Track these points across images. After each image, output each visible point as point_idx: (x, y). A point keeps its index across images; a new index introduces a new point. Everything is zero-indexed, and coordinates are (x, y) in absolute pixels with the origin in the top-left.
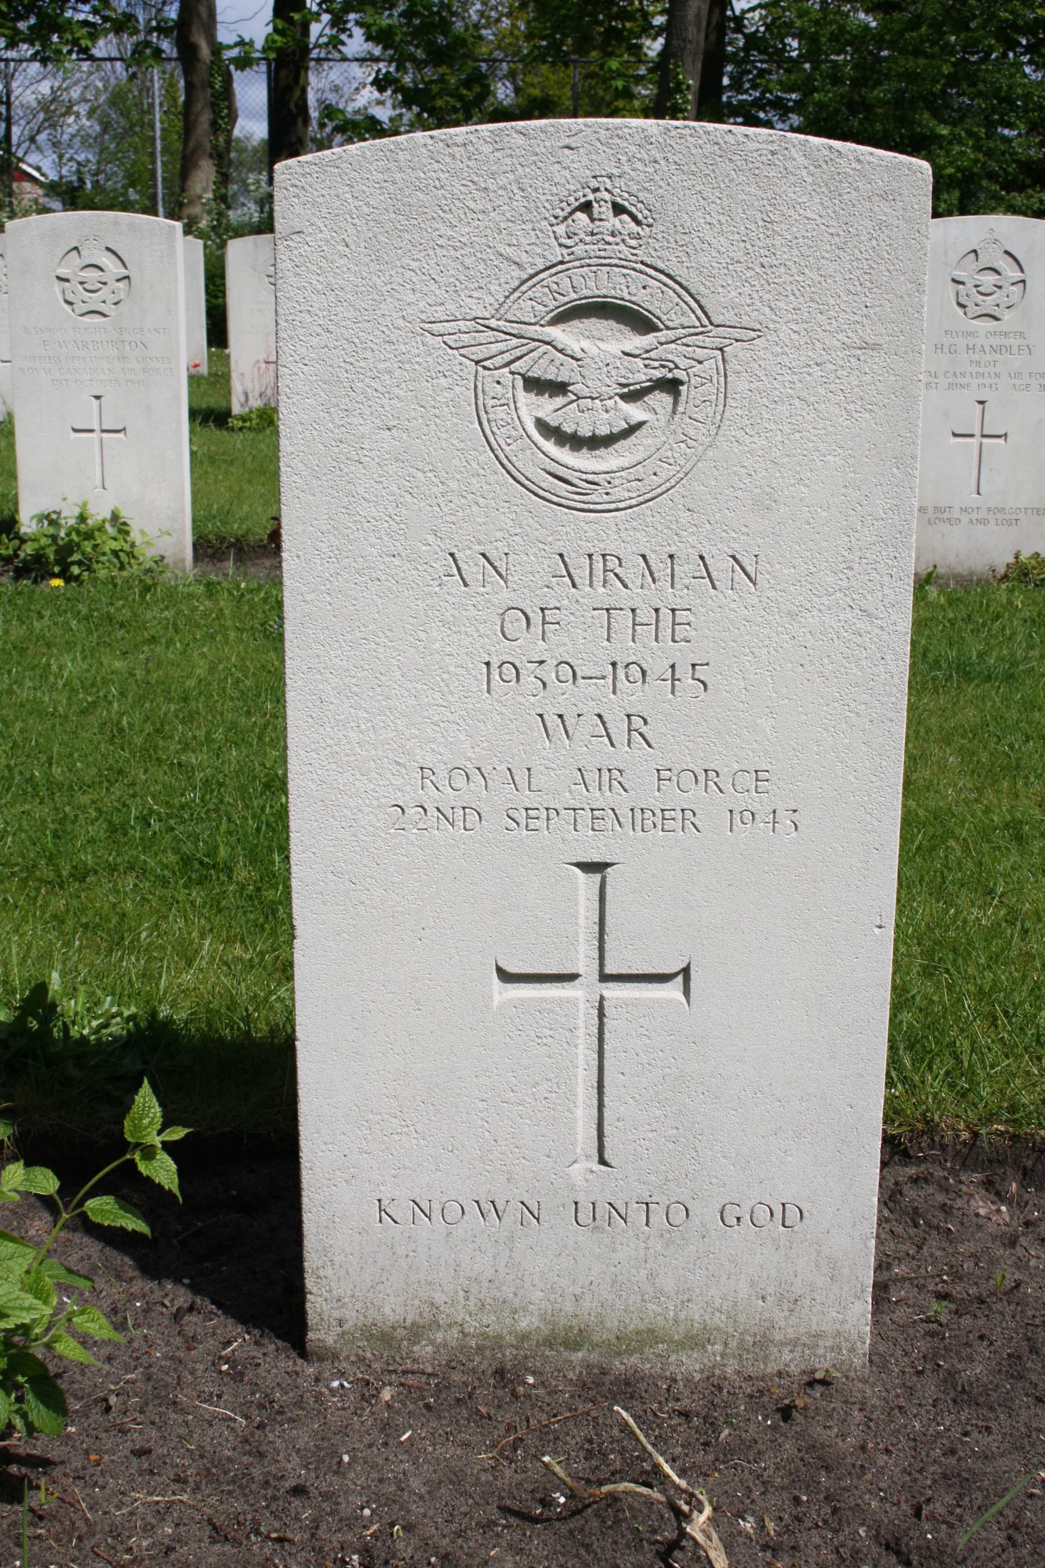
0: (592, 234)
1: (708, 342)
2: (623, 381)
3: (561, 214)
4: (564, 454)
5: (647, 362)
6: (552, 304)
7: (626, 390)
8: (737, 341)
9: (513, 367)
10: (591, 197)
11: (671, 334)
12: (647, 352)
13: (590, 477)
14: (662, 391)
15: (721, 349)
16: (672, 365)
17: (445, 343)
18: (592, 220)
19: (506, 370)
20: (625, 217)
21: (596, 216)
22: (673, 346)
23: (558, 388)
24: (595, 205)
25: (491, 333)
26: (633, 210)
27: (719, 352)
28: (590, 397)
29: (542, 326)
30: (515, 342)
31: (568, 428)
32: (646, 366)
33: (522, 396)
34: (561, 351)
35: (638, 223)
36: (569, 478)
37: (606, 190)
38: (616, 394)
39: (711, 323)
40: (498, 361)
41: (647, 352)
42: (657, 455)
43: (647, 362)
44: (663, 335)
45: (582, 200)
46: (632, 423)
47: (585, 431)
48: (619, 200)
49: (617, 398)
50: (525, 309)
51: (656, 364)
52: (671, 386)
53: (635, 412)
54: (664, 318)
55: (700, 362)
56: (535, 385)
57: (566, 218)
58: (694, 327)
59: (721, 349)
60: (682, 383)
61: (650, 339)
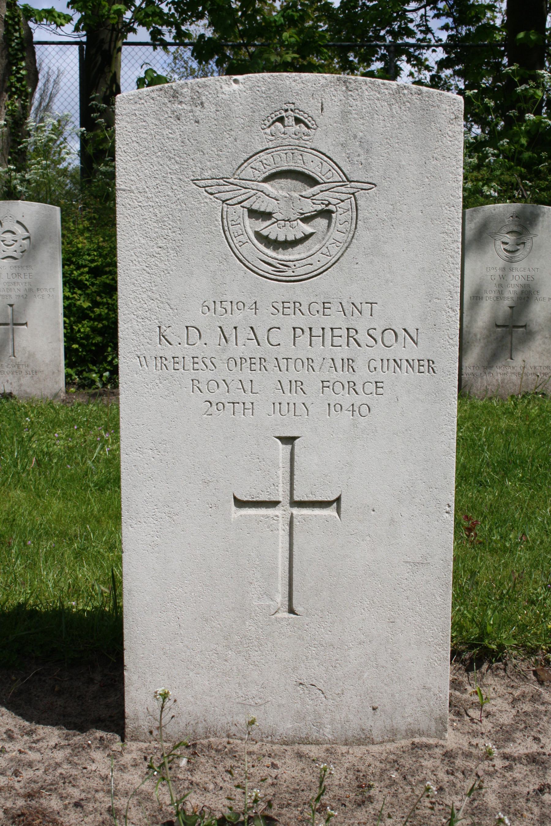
0: (284, 133)
2: (301, 211)
3: (268, 124)
4: (270, 252)
5: (314, 201)
7: (303, 216)
8: (362, 189)
10: (284, 114)
12: (314, 195)
14: (321, 218)
15: (353, 194)
17: (206, 191)
18: (284, 126)
19: (239, 205)
20: (302, 125)
21: (286, 124)
22: (327, 192)
23: (266, 216)
24: (286, 119)
25: (232, 186)
26: (306, 121)
28: (284, 220)
29: (259, 182)
30: (244, 191)
31: (272, 237)
32: (314, 203)
33: (247, 221)
34: (268, 195)
35: (308, 127)
36: (272, 263)
37: (292, 110)
38: (298, 218)
39: (348, 180)
40: (235, 201)
41: (314, 195)
42: (320, 251)
43: (314, 201)
45: (280, 116)
46: (307, 234)
47: (281, 238)
48: (298, 116)
50: (248, 172)
52: (326, 214)
53: (308, 229)
54: (323, 177)
55: (342, 201)
56: (254, 214)
57: (269, 127)
58: (340, 182)
59: (353, 194)
60: (333, 212)
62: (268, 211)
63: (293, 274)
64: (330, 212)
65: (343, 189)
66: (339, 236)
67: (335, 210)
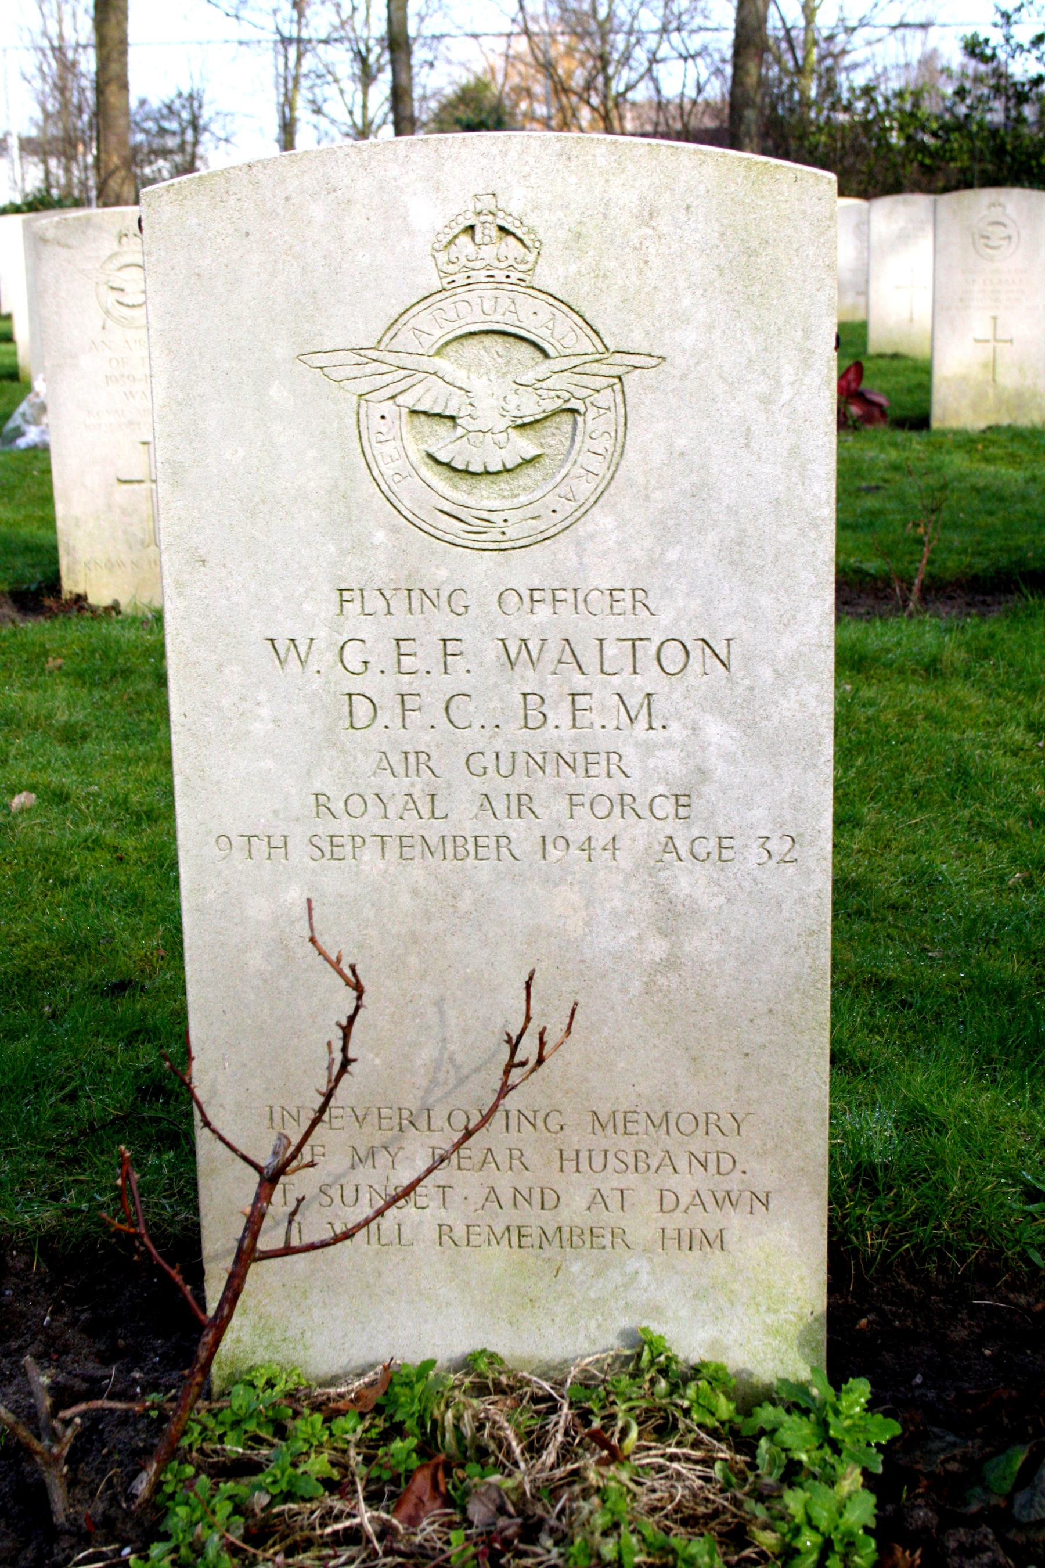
1: (604, 369)
4: (457, 493)
5: (539, 392)
6: (438, 333)
7: (519, 422)
9: (400, 400)
11: (566, 363)
13: (485, 515)
16: (567, 396)
20: (511, 239)
24: (478, 230)
27: (616, 380)
44: (557, 365)
49: (510, 430)
51: (553, 394)
54: (559, 346)
59: (620, 378)
61: (544, 367)
62: (447, 413)
63: (500, 537)
64: (573, 411)
65: (595, 368)
66: (597, 465)
67: (582, 410)
